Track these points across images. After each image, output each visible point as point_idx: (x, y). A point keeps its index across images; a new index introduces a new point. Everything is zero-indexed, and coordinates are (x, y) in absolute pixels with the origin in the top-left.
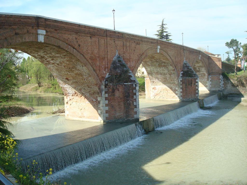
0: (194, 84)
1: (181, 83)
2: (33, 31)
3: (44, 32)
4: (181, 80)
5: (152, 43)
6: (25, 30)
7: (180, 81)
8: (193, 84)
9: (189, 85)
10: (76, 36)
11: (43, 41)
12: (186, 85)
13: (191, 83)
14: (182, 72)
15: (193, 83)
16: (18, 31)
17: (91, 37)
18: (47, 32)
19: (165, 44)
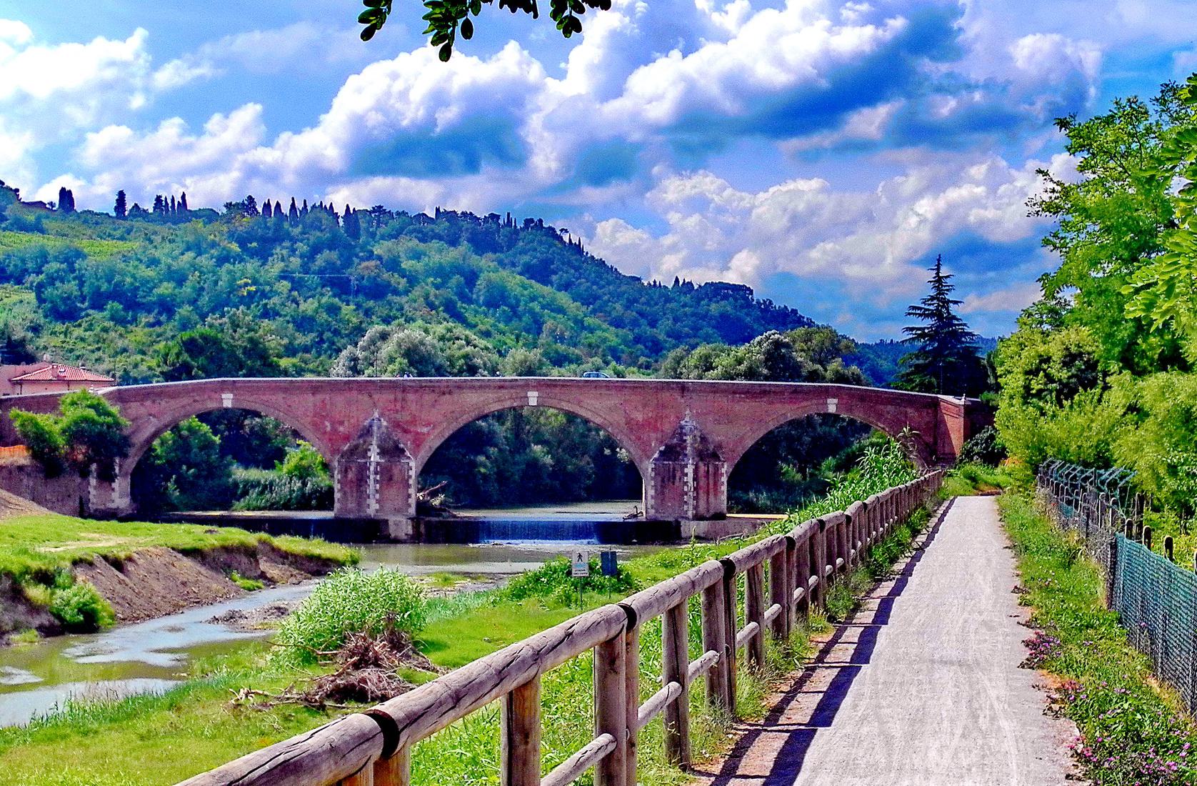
0: (680, 479)
1: (653, 475)
2: (217, 396)
3: (231, 396)
4: (653, 466)
5: (501, 387)
6: (206, 397)
7: (650, 470)
8: (677, 478)
9: (669, 480)
10: (284, 395)
11: (230, 406)
12: (663, 481)
13: (674, 477)
14: (662, 448)
15: (678, 474)
16: (197, 398)
17: (313, 394)
18: (235, 395)
19: (563, 386)
